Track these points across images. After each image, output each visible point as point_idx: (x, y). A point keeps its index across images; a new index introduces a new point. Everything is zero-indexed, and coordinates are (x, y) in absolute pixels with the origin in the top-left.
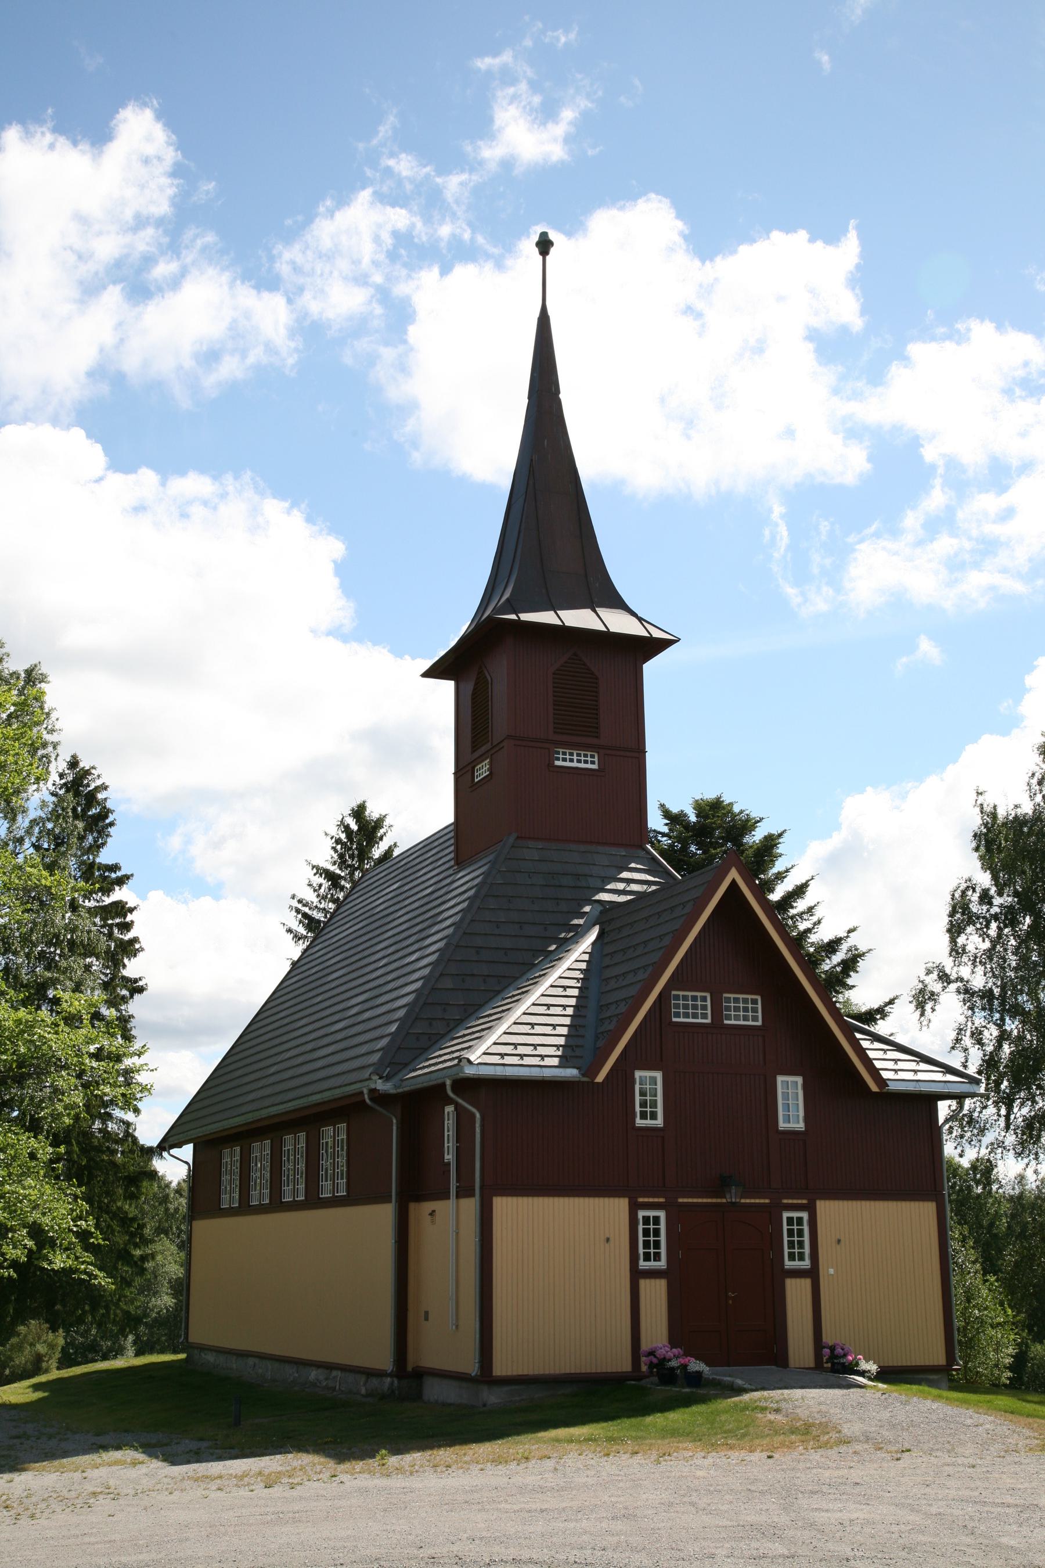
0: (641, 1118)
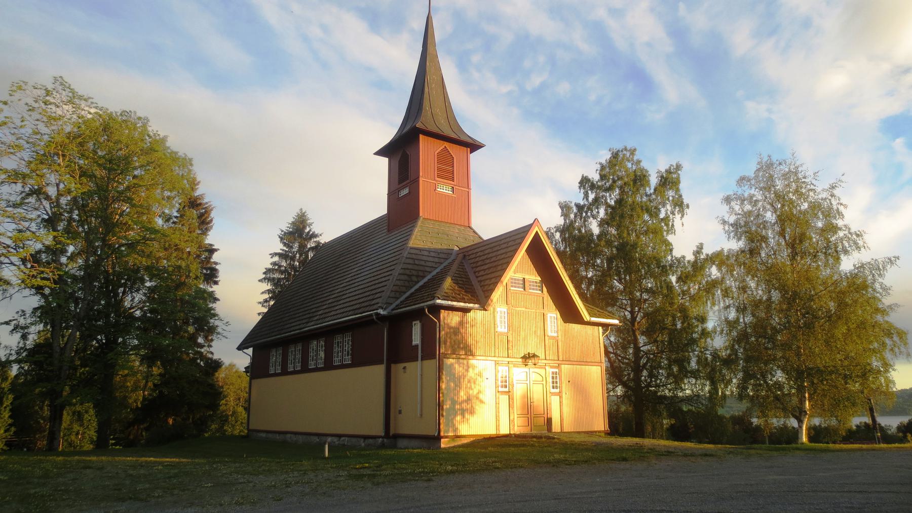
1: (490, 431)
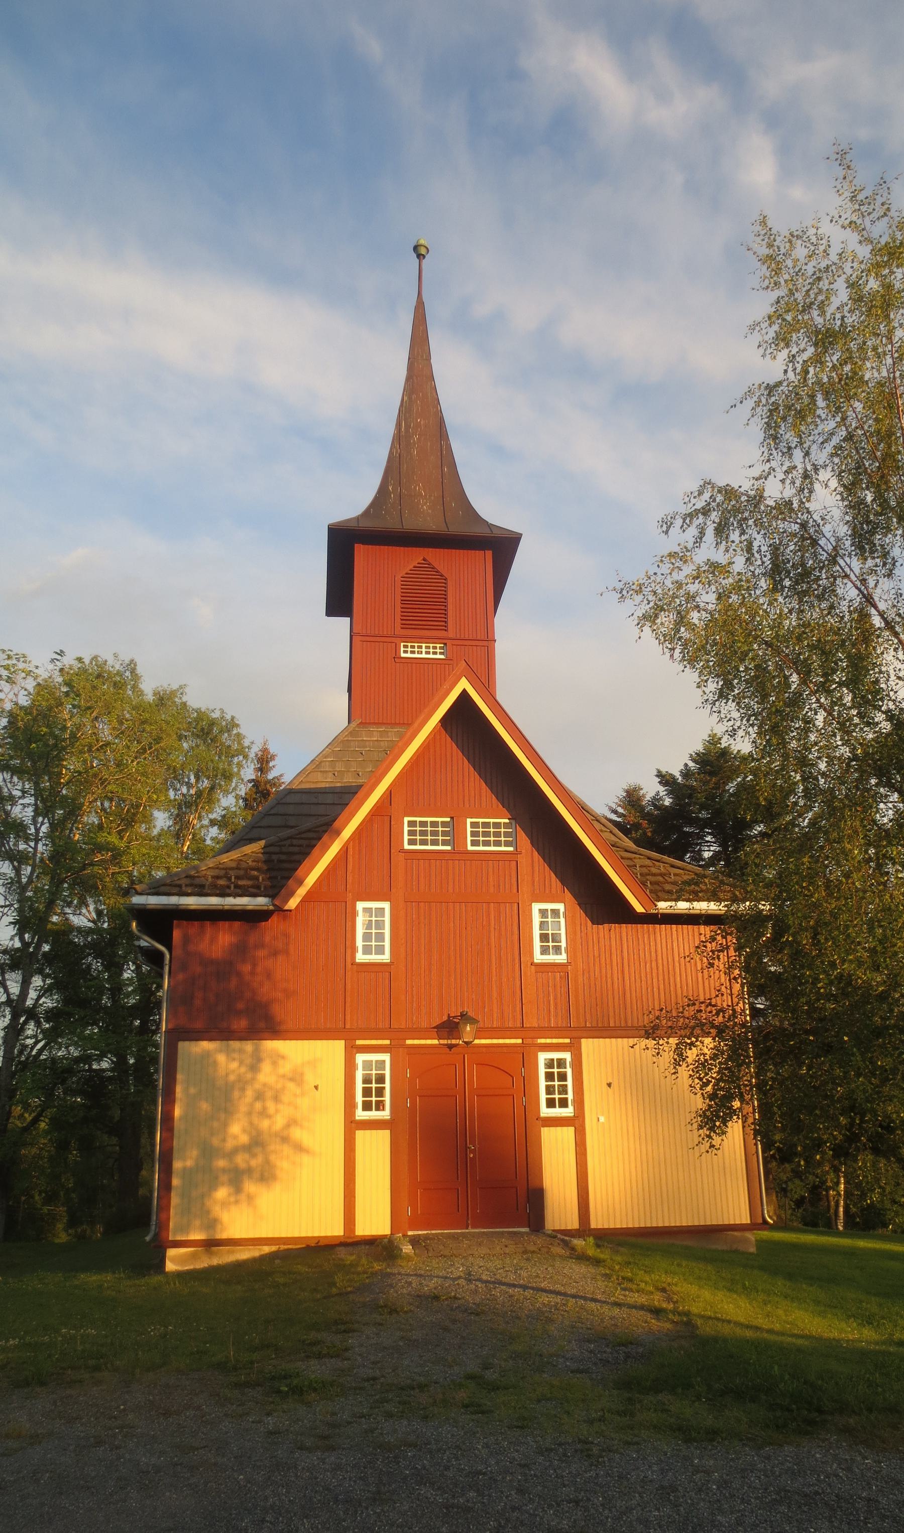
0: (364, 953)
1: (328, 1225)
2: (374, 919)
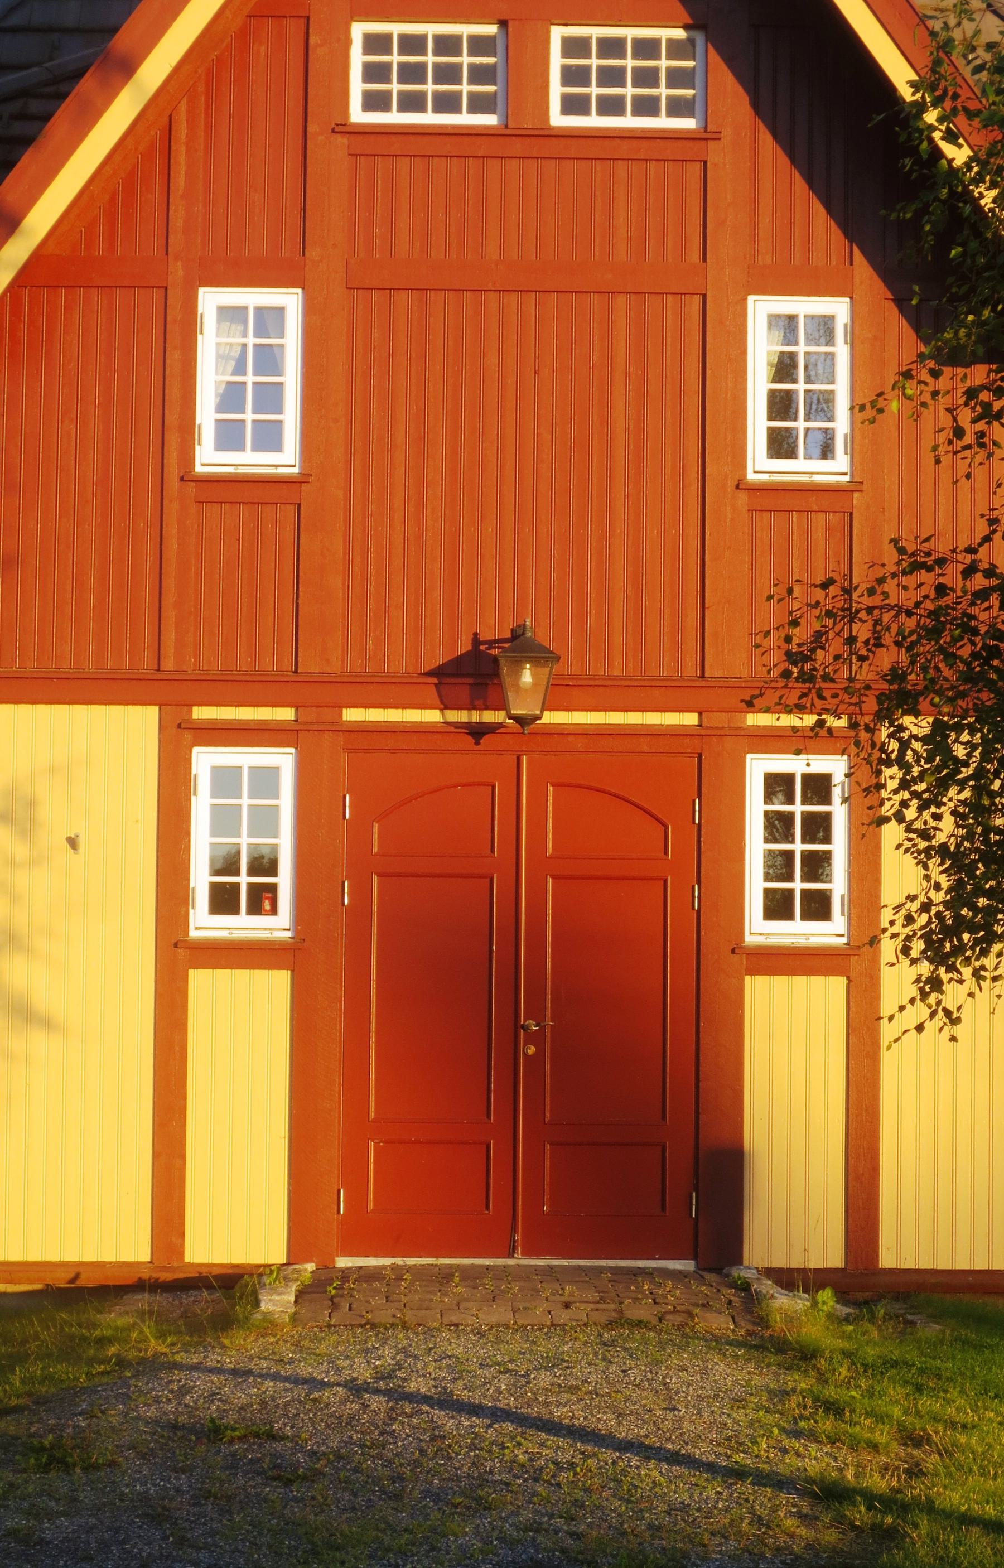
2: (251, 340)
